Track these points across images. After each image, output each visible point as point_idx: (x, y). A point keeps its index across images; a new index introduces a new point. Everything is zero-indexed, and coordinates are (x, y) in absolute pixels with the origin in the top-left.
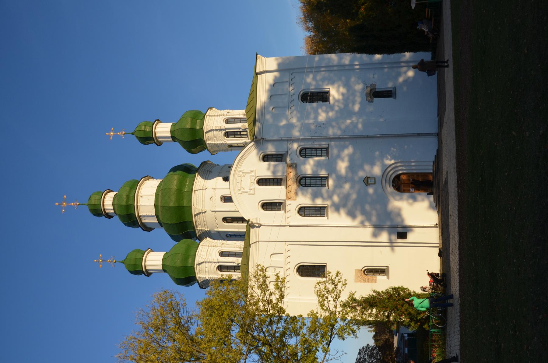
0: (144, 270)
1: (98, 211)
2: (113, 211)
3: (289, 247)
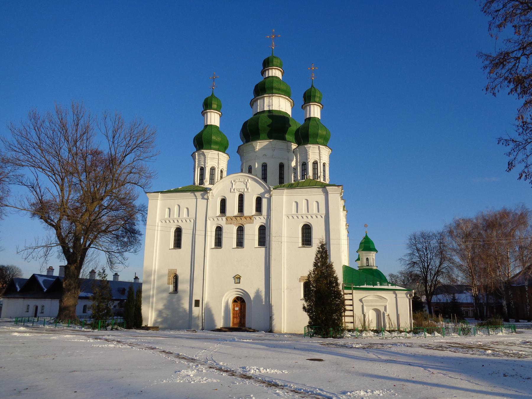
1: (267, 64)
2: (267, 76)
3: (192, 221)
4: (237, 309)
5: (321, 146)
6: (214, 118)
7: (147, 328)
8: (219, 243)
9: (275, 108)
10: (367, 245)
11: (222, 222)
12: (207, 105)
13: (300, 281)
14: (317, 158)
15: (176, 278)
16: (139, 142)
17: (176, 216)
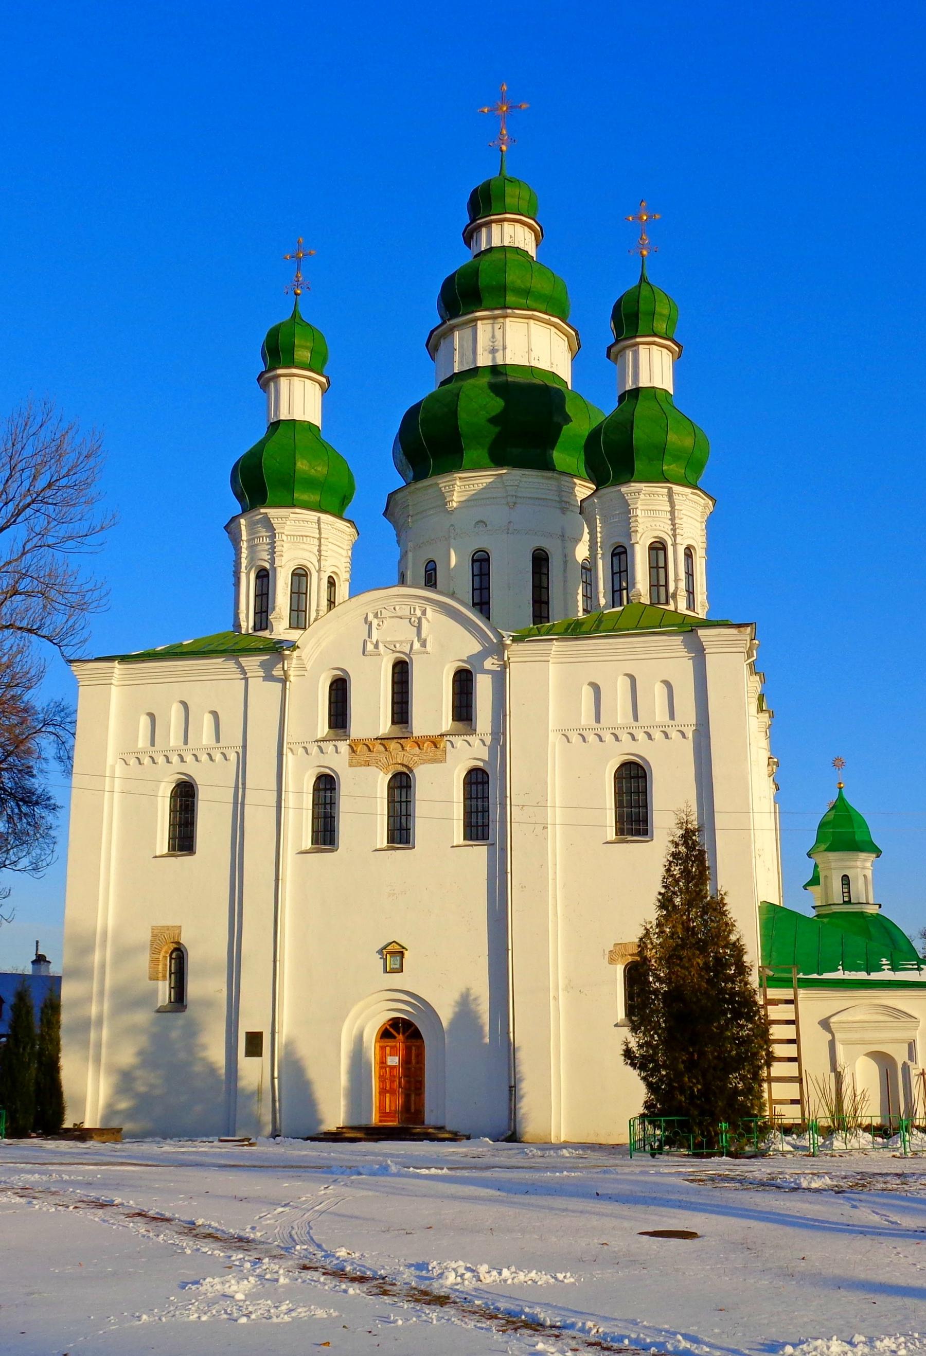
0: (280, 371)
1: (483, 204)
3: (233, 757)
4: (393, 1061)
5: (676, 488)
6: (301, 398)
7: (81, 1134)
8: (325, 832)
9: (515, 356)
10: (842, 833)
11: (337, 759)
12: (277, 353)
13: (612, 961)
14: (662, 530)
15: (179, 956)
16: (41, 484)
17: (175, 740)
